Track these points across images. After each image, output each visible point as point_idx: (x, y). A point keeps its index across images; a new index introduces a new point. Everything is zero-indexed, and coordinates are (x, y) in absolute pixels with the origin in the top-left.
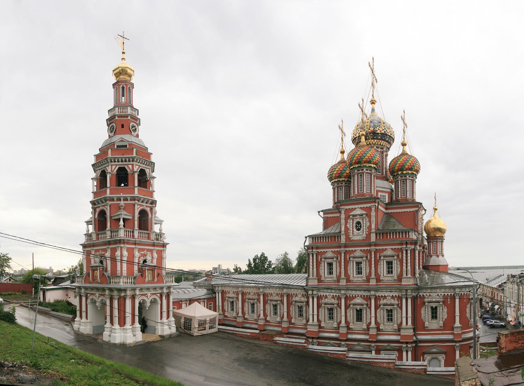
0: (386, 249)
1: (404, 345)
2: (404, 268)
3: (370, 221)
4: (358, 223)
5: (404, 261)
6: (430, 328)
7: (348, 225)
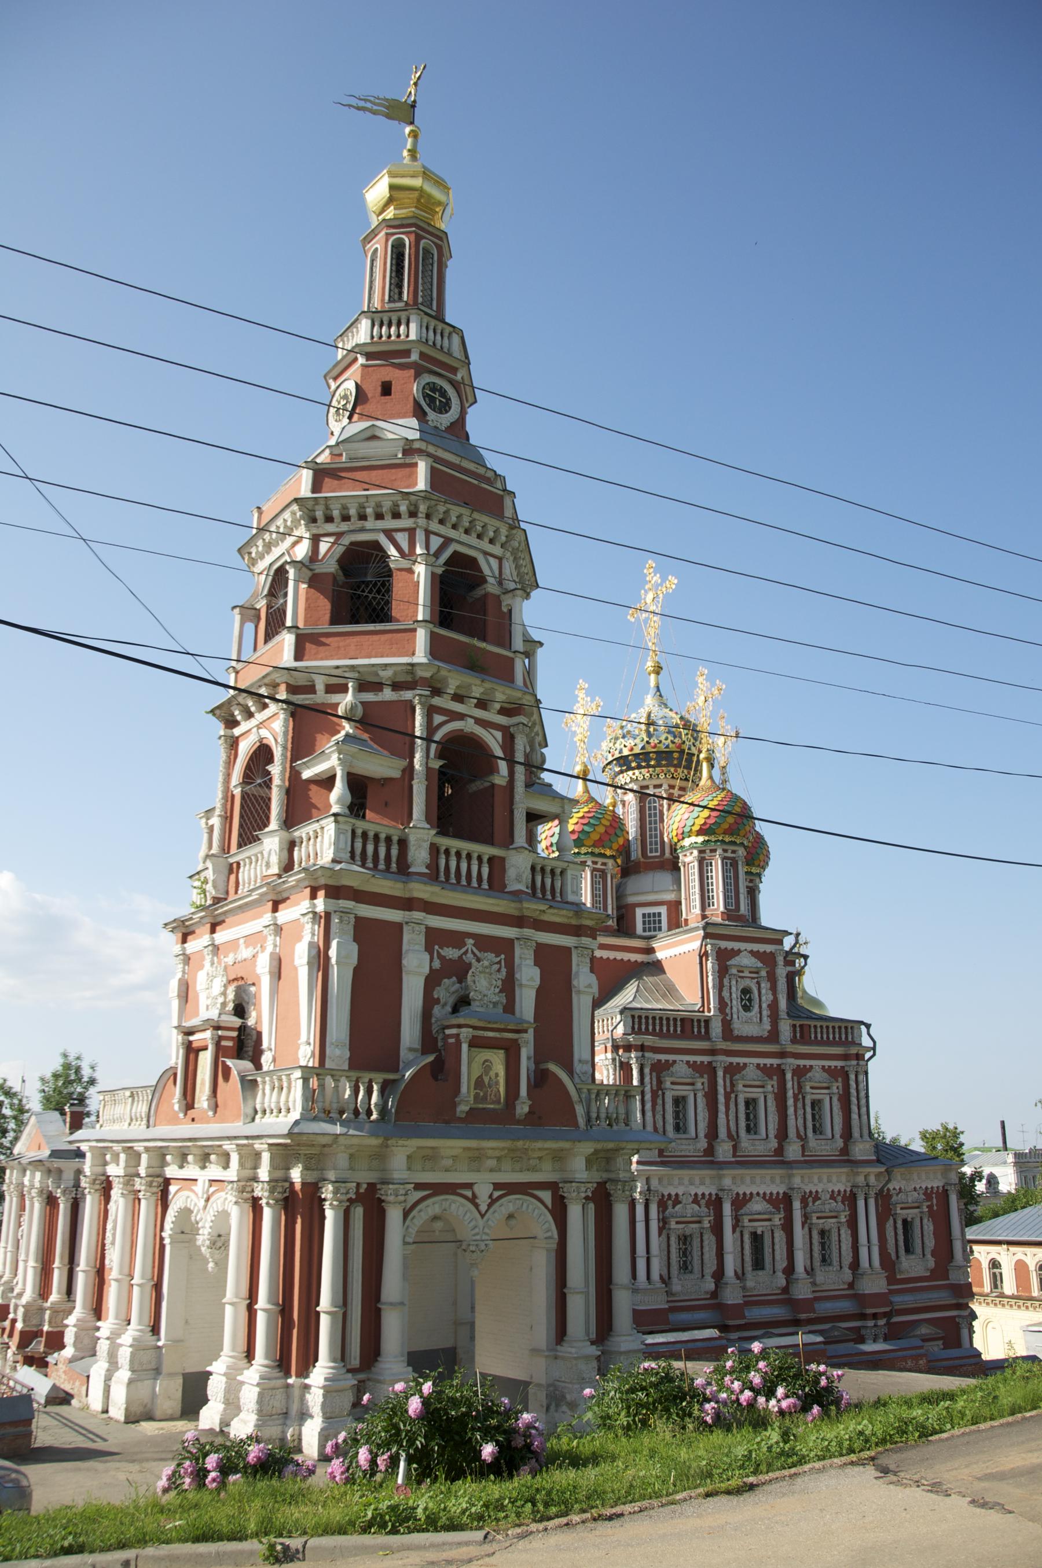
0: (811, 1066)
1: (871, 1323)
2: (855, 1116)
3: (774, 989)
4: (746, 991)
5: (854, 1100)
6: (913, 1275)
7: (725, 994)
